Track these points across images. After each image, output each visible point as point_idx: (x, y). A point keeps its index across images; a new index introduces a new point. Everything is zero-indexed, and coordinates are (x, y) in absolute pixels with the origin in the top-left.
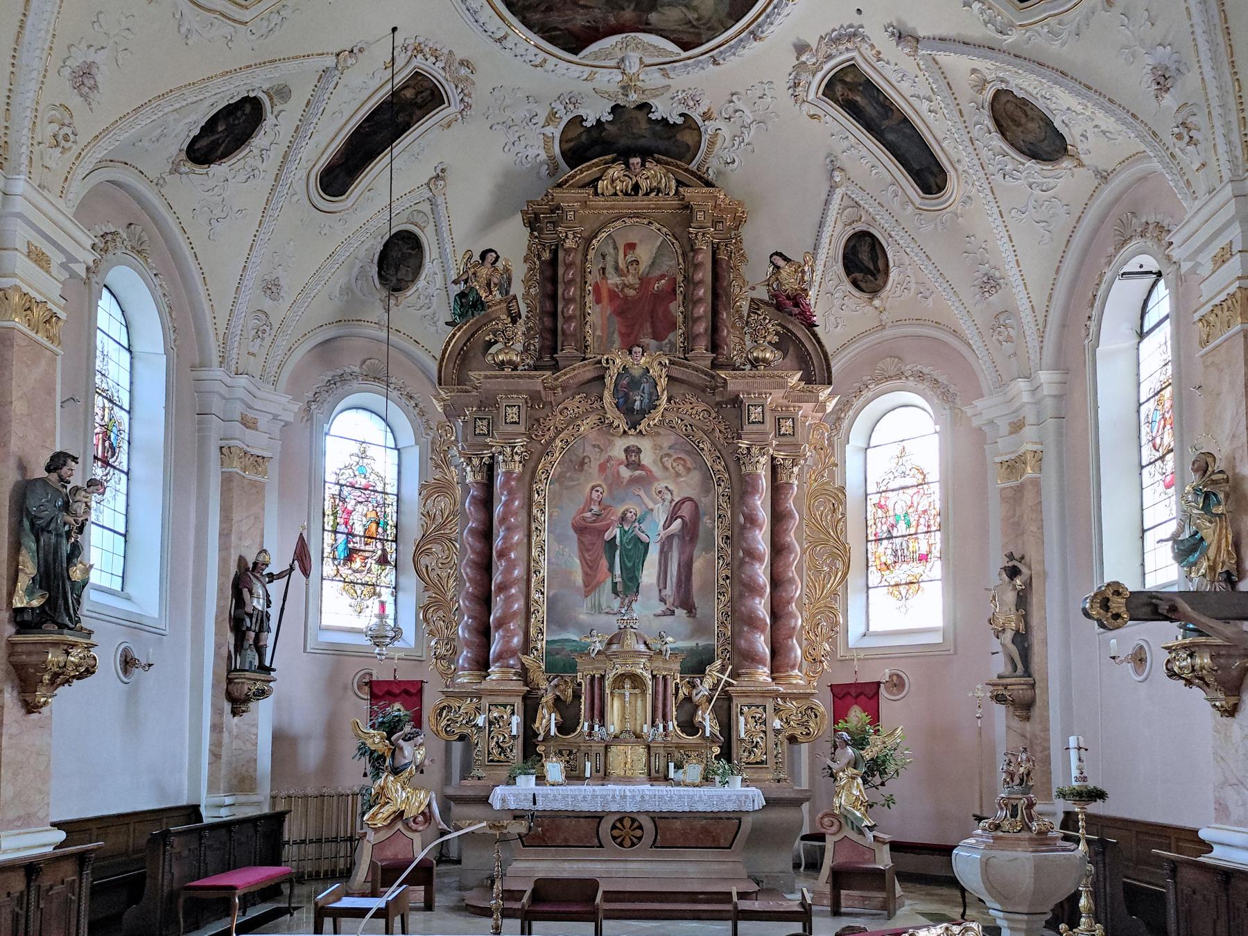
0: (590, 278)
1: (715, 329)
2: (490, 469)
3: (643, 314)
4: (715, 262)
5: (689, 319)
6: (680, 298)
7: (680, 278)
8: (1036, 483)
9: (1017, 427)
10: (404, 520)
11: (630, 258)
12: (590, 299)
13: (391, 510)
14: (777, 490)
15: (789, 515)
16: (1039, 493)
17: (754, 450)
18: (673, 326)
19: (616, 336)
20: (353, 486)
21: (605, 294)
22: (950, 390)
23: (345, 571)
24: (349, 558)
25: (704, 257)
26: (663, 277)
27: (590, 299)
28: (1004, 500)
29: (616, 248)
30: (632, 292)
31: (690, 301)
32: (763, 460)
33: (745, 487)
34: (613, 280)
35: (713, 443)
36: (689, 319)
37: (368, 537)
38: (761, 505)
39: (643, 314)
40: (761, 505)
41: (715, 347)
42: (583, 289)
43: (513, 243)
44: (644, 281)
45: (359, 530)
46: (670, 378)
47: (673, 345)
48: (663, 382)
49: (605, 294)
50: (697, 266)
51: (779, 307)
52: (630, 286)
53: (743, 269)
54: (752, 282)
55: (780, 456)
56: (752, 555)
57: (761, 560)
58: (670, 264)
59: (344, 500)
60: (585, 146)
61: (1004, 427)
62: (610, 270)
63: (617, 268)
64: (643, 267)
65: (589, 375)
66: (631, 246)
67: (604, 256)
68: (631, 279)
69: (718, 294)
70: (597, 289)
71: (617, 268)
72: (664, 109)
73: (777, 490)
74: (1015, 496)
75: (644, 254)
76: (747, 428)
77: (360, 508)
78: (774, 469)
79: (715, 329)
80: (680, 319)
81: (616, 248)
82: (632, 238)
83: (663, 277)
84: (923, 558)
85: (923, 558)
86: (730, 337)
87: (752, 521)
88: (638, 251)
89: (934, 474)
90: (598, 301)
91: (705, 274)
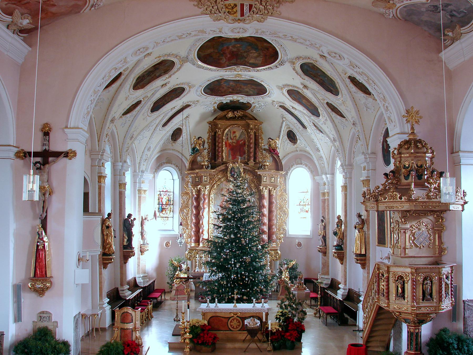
0: (224, 141)
1: (255, 153)
2: (199, 192)
3: (237, 149)
4: (255, 136)
5: (249, 151)
6: (246, 146)
7: (246, 141)
8: (328, 199)
9: (325, 184)
10: (175, 199)
11: (234, 135)
12: (224, 146)
13: (172, 196)
14: (270, 196)
15: (273, 203)
16: (328, 202)
17: (264, 188)
18: (245, 153)
19: (231, 156)
20: (163, 191)
21: (228, 144)
22: (314, 172)
23: (161, 214)
24: (162, 211)
25: (253, 136)
26: (242, 140)
27: (224, 146)
28: (322, 202)
29: (231, 133)
30: (234, 144)
31: (249, 147)
32: (266, 191)
33: (261, 197)
34: (230, 141)
35: (255, 184)
36: (249, 151)
37: (166, 204)
38: (266, 203)
39: (237, 149)
40: (266, 203)
41: (255, 160)
42: (222, 143)
43: (204, 133)
44: (238, 141)
45: (164, 203)
46: (243, 168)
47: (245, 158)
48: (242, 170)
49: (228, 144)
50: (251, 139)
51: (270, 151)
52: (234, 143)
53: (263, 136)
54: (264, 144)
55: (271, 188)
56: (263, 215)
57: (265, 216)
58: (245, 137)
59: (161, 195)
60: (222, 107)
61: (323, 184)
62: (229, 138)
63: (231, 138)
64: (237, 138)
65: (224, 168)
66: (234, 132)
67: (227, 135)
68: (234, 141)
69: (256, 144)
70: (226, 143)
71: (231, 138)
72: (241, 101)
73: (270, 196)
74: (324, 201)
75: (238, 134)
76: (262, 183)
77: (165, 197)
78: (270, 191)
79: (255, 153)
80: (246, 151)
81: (231, 133)
82: (235, 130)
83: (242, 140)
84: (307, 212)
85: (307, 212)
86: (259, 154)
87: (263, 206)
88: (236, 133)
89: (309, 191)
90: (226, 146)
91: (252, 141)
